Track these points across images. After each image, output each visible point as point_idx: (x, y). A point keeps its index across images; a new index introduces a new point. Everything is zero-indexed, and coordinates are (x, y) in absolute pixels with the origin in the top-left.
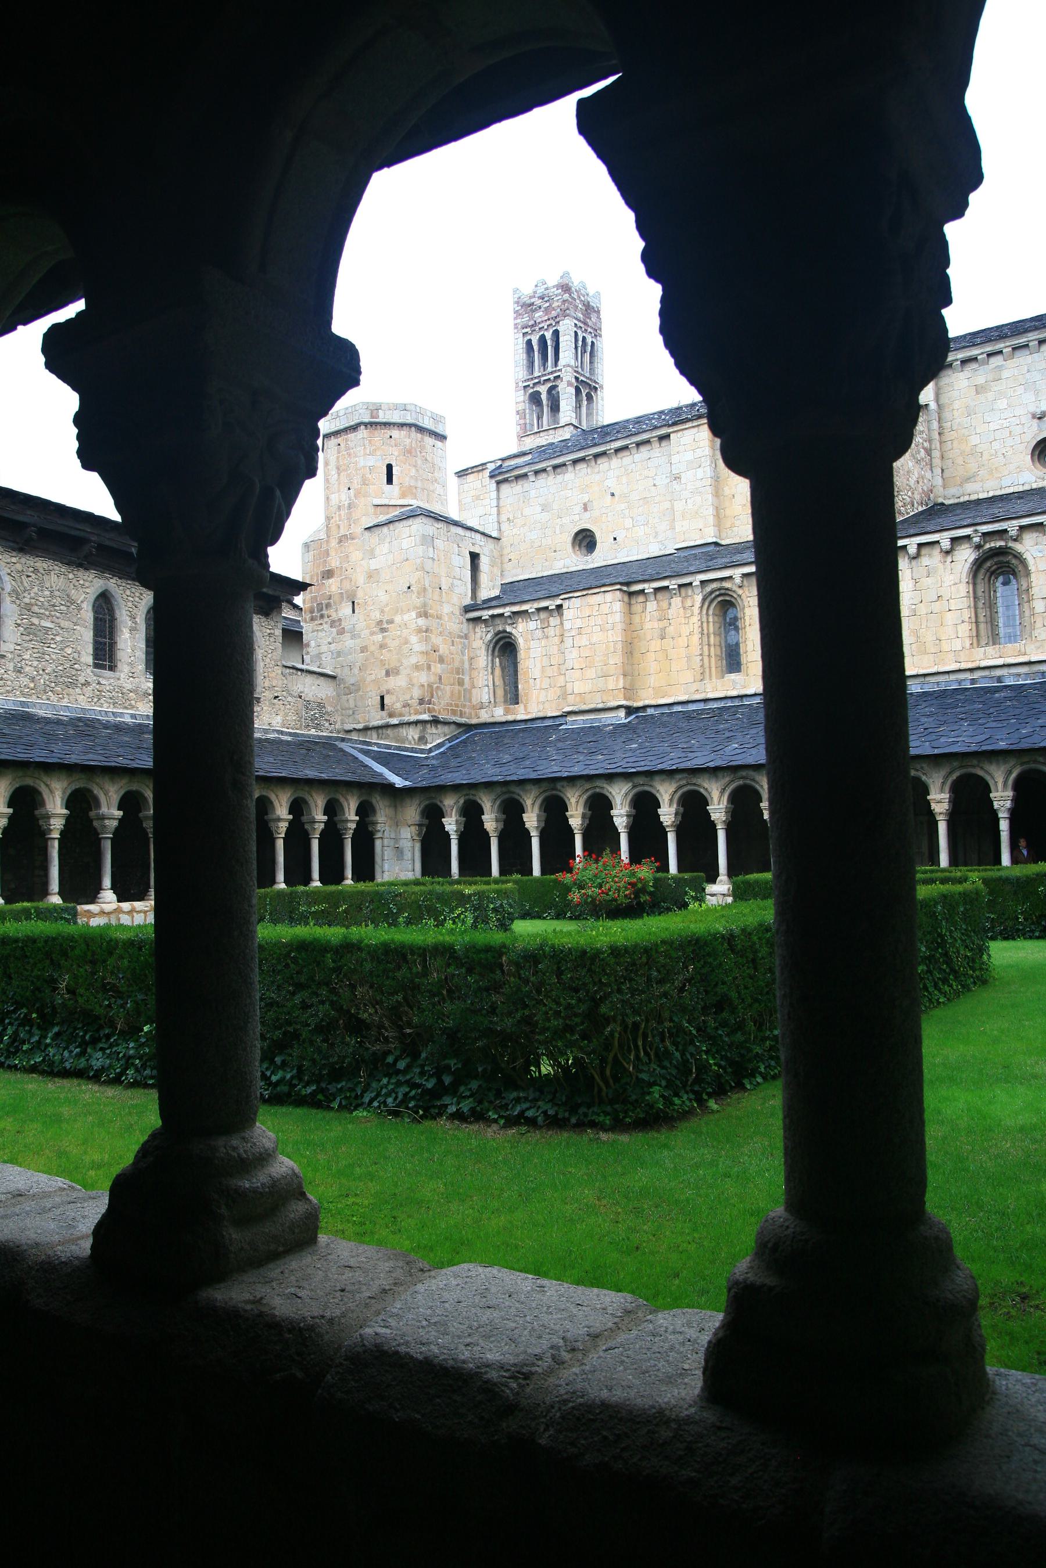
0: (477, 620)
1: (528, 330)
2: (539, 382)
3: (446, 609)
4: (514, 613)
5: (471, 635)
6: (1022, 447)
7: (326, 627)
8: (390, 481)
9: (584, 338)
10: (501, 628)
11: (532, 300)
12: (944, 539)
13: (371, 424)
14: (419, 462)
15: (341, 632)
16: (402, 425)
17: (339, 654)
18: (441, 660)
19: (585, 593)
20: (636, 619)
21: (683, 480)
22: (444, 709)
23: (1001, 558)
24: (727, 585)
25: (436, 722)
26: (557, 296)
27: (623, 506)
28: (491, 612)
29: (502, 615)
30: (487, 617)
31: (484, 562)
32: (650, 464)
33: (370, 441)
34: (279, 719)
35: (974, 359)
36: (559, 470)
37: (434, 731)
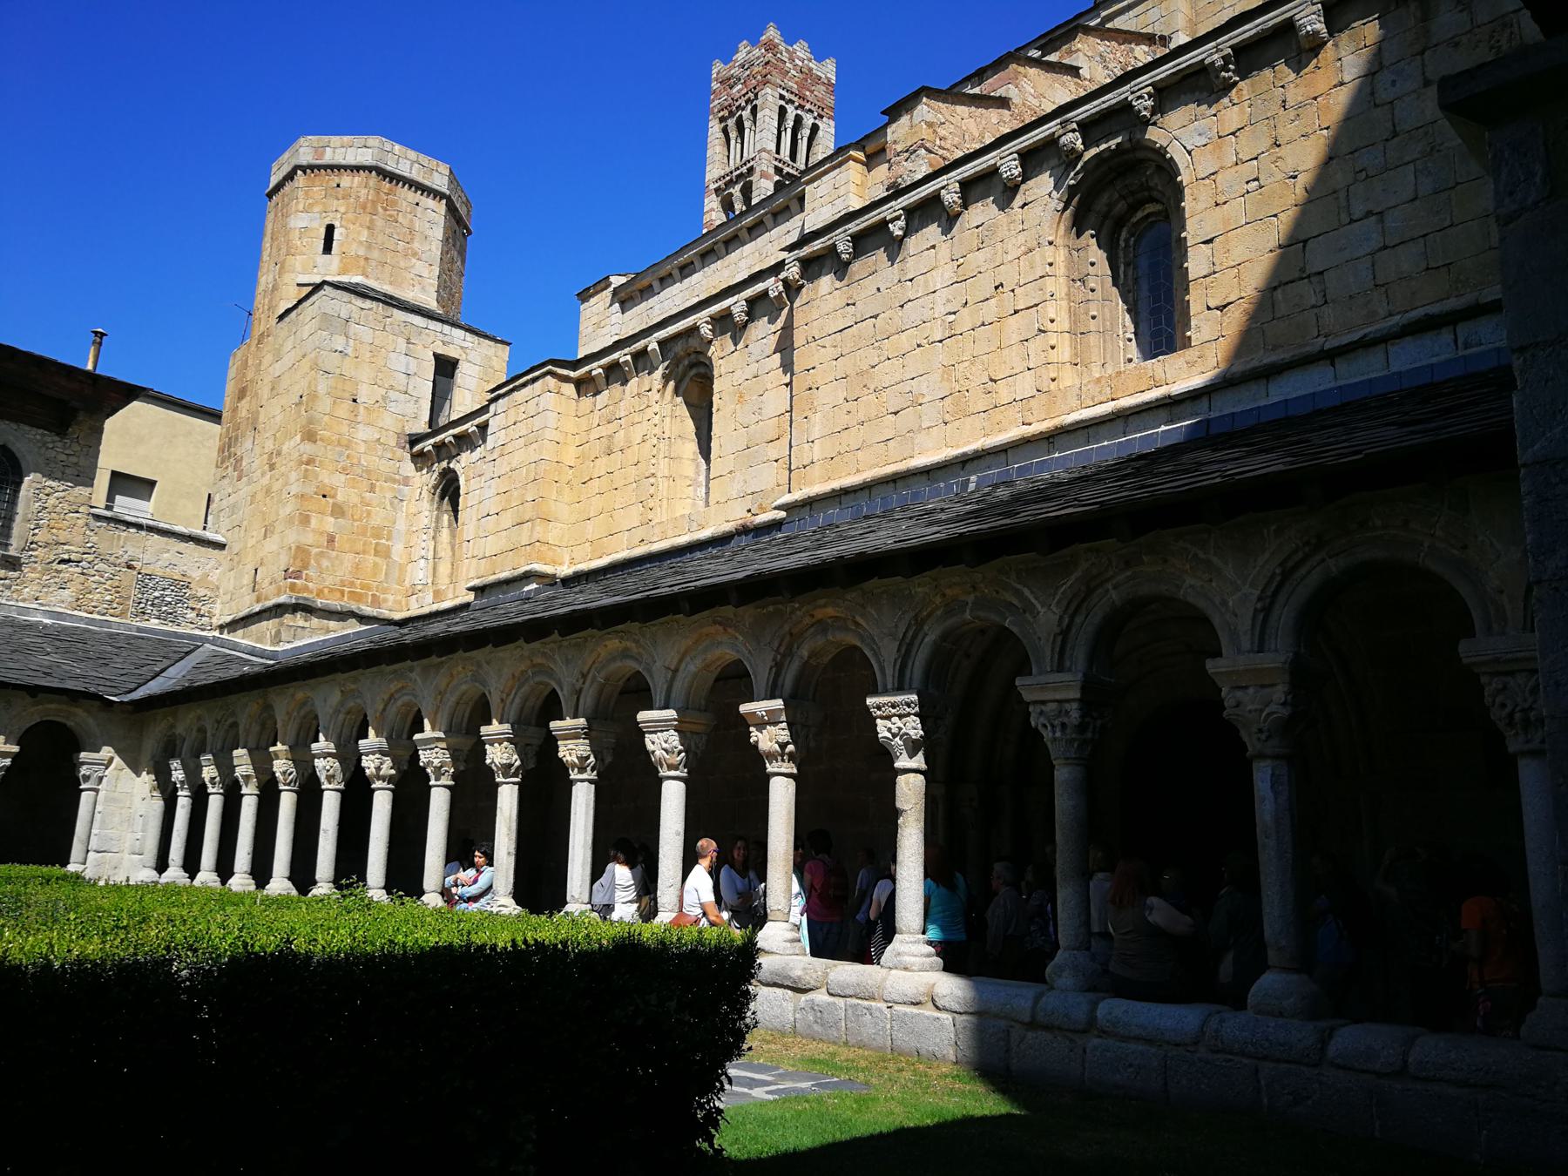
1: (726, 113)
2: (731, 180)
4: (454, 436)
8: (328, 248)
9: (798, 121)
10: (444, 464)
11: (732, 72)
13: (312, 167)
14: (379, 223)
16: (357, 168)
19: (511, 386)
22: (331, 591)
24: (694, 343)
25: (307, 609)
26: (758, 58)
30: (430, 448)
33: (306, 193)
36: (686, 271)
37: (301, 623)
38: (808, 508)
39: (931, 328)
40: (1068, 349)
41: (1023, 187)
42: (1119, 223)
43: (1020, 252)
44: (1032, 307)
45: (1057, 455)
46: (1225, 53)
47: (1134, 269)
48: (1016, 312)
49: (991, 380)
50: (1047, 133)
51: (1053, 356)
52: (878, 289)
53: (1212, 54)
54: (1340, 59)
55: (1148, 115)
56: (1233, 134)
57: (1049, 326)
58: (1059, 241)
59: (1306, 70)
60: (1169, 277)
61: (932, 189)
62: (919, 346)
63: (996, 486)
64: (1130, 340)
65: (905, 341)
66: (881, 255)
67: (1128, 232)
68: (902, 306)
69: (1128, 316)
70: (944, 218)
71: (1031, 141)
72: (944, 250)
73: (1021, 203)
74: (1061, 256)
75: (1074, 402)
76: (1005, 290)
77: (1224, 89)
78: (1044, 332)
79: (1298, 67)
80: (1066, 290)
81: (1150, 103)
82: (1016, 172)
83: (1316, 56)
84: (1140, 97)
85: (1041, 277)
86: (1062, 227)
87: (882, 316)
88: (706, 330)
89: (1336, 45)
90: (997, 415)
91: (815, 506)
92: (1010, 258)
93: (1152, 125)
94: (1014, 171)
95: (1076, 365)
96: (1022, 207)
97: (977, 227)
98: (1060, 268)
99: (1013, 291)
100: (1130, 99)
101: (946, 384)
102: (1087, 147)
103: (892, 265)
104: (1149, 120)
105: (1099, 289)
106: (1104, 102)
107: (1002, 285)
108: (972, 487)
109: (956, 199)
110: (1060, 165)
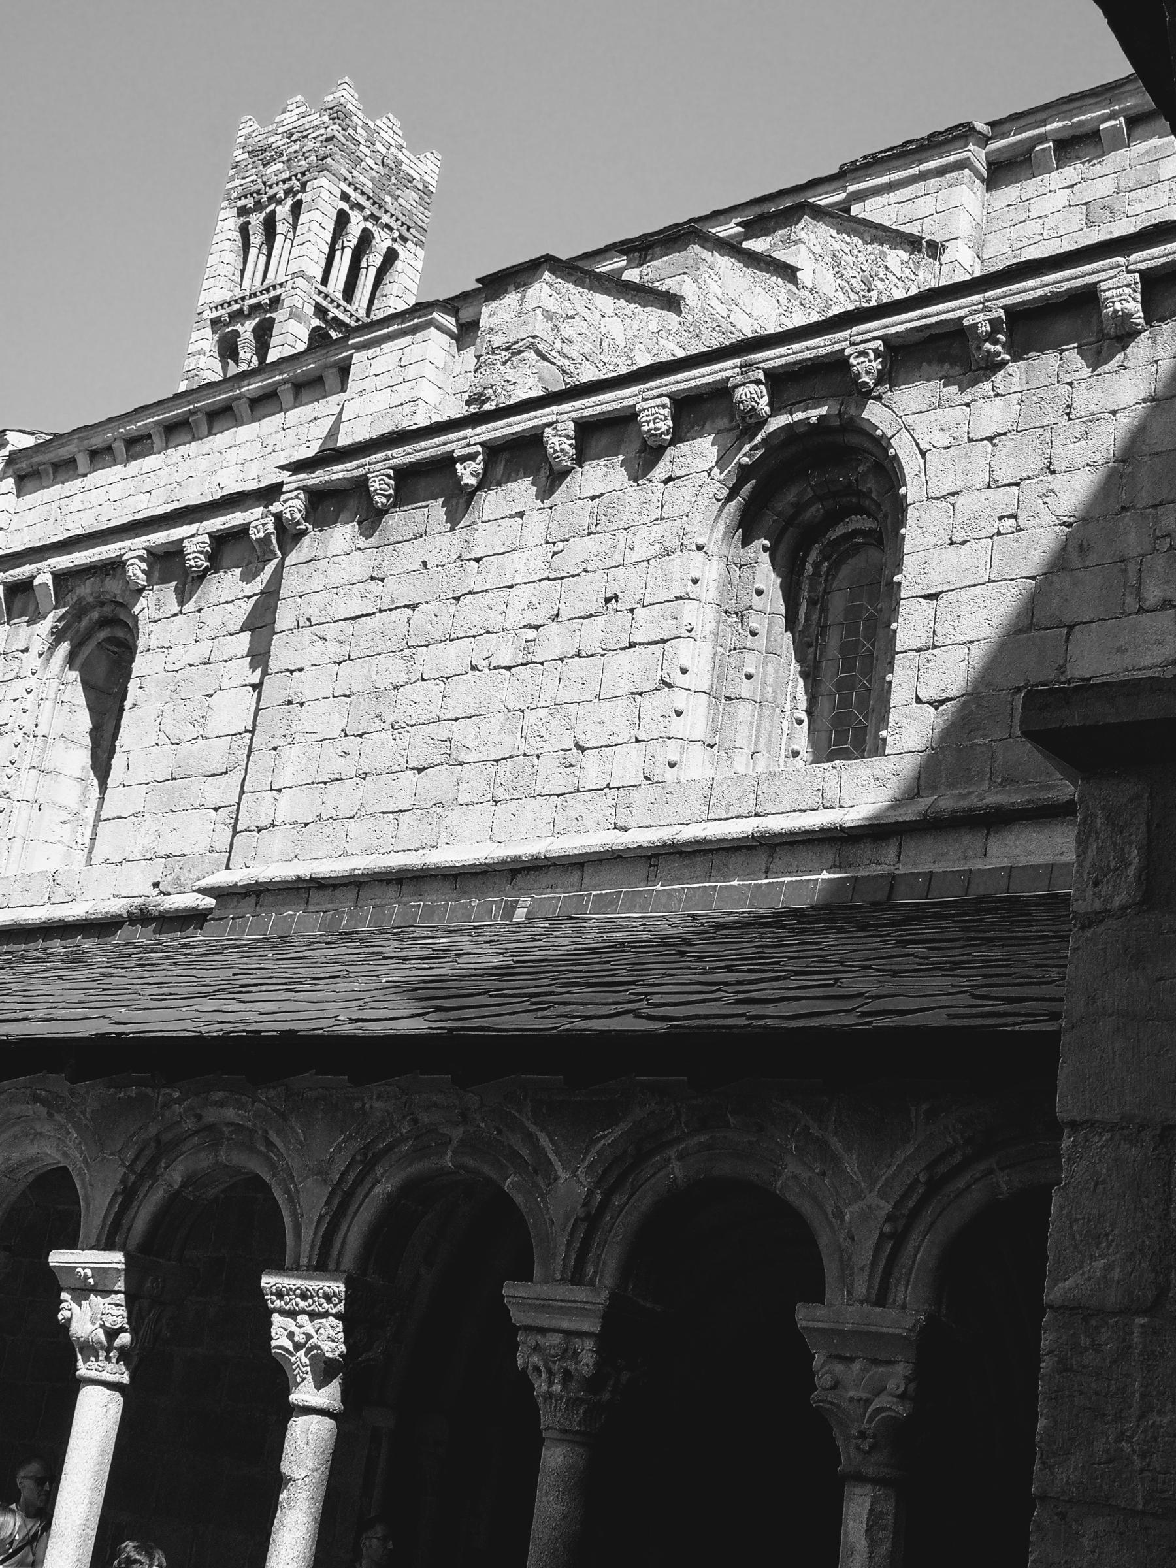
38: (253, 900)
39: (498, 645)
40: (704, 719)
41: (671, 451)
42: (809, 536)
43: (651, 552)
44: (656, 643)
45: (659, 887)
46: (996, 315)
47: (822, 610)
48: (632, 645)
49: (578, 747)
50: (718, 377)
51: (677, 727)
52: (425, 563)
53: (975, 312)
54: (1156, 362)
55: (871, 383)
56: (990, 439)
57: (678, 679)
58: (712, 548)
59: (1106, 367)
60: (871, 634)
61: (532, 423)
62: (474, 668)
63: (555, 922)
64: (800, 722)
66: (436, 509)
67: (821, 552)
68: (457, 599)
69: (801, 681)
70: (544, 473)
71: (693, 384)
72: (537, 524)
73: (664, 476)
74: (711, 571)
75: (699, 808)
76: (621, 606)
77: (986, 368)
78: (669, 686)
79: (1096, 359)
80: (714, 624)
81: (876, 365)
82: (663, 426)
83: (1124, 348)
84: (863, 354)
85: (677, 599)
86: (721, 528)
87: (421, 607)
89: (1153, 339)
90: (577, 804)
91: (267, 899)
92: (634, 556)
93: (874, 398)
94: (660, 424)
95: (712, 747)
96: (666, 481)
97: (593, 498)
98: (709, 591)
99: (632, 611)
100: (847, 353)
101: (506, 738)
102: (775, 410)
103: (452, 529)
104: (872, 391)
105: (763, 632)
106: (808, 349)
107: (616, 597)
108: (520, 914)
109: (566, 447)
110: (730, 430)
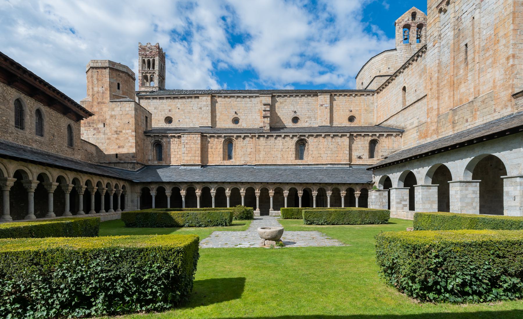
0: (150, 136)
3: (140, 131)
4: (162, 136)
5: (146, 140)
6: (290, 118)
7: (92, 130)
12: (291, 135)
15: (100, 132)
17: (98, 139)
18: (139, 146)
20: (204, 143)
21: (203, 109)
23: (302, 141)
27: (182, 113)
28: (154, 134)
29: (158, 136)
31: (149, 119)
32: (191, 103)
34: (80, 157)
35: (280, 96)
65: (275, 150)
88: (235, 137)
